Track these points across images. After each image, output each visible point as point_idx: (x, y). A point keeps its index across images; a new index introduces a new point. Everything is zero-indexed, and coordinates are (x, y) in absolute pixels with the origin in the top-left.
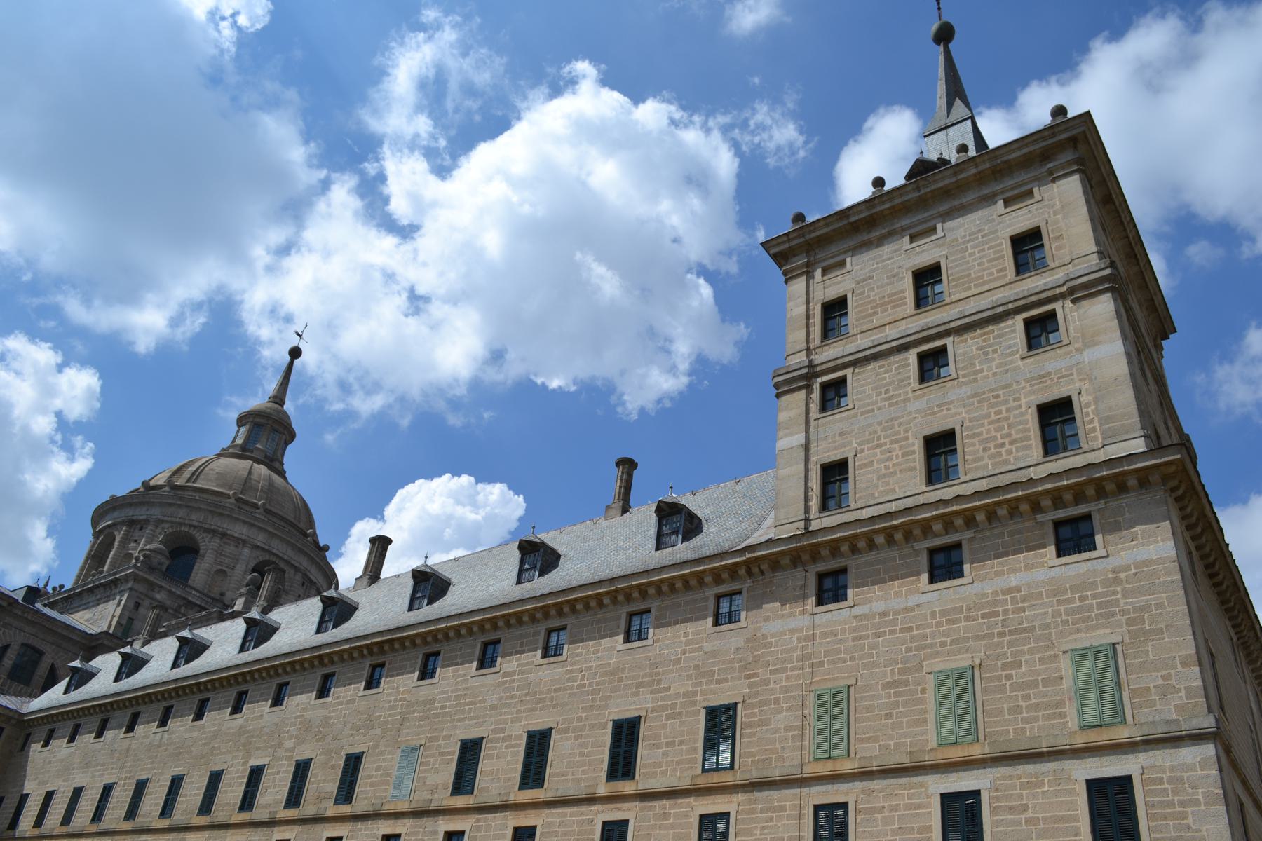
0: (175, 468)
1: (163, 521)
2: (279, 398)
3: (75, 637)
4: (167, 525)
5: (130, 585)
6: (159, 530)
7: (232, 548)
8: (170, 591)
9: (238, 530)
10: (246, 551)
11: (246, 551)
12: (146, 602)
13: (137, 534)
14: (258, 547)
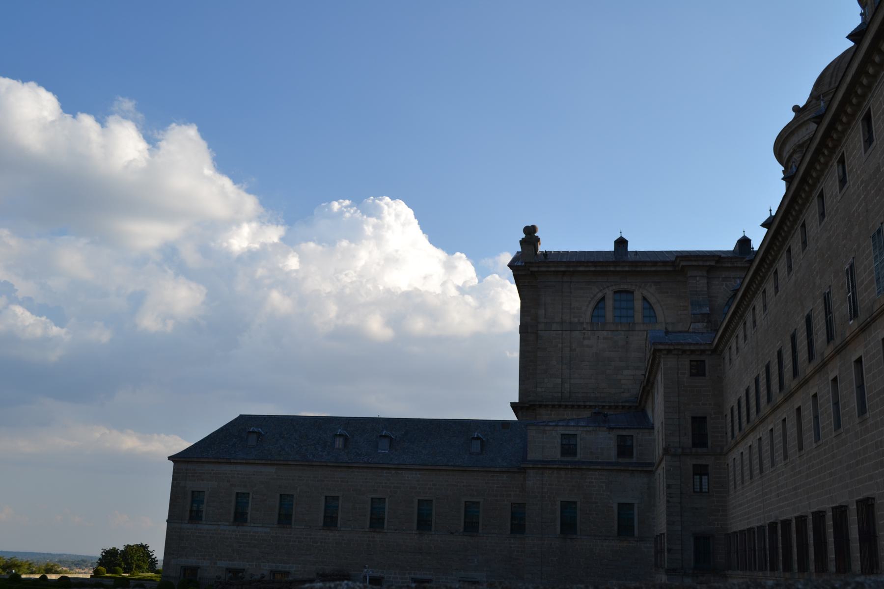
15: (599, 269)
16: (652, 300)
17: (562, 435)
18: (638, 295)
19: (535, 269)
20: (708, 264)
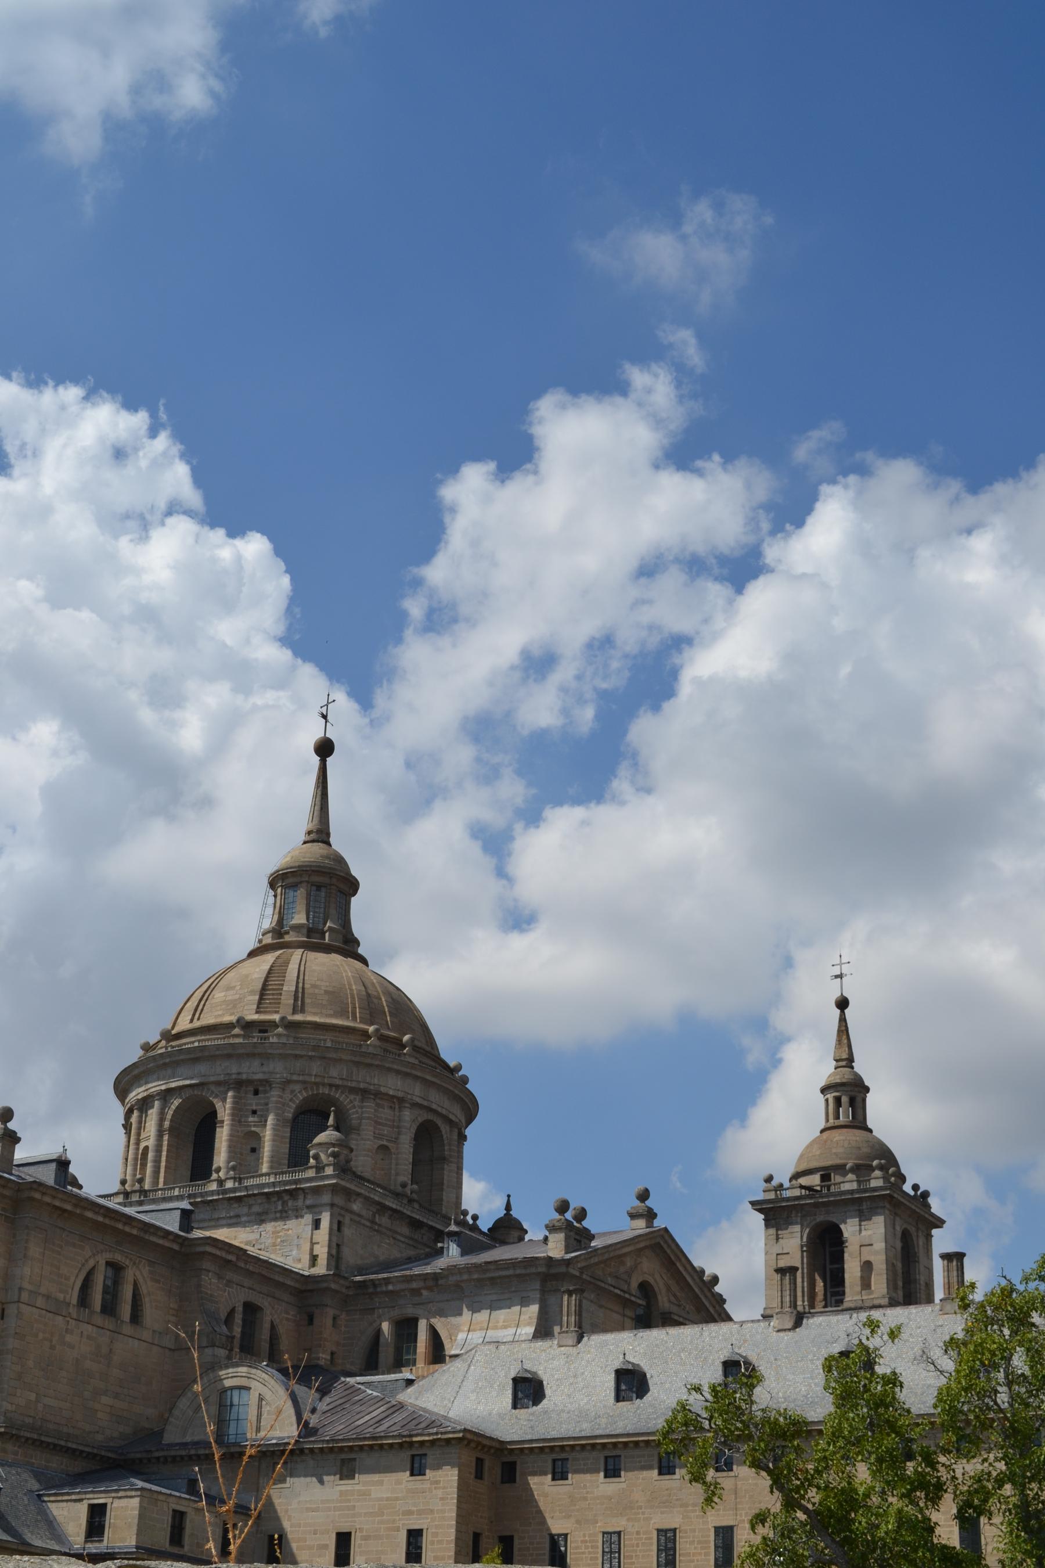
0: (260, 986)
1: (289, 1082)
2: (321, 834)
3: (289, 1282)
4: (297, 1087)
5: (326, 1198)
6: (287, 1096)
7: (387, 1111)
8: (367, 1199)
9: (392, 1085)
10: (407, 1114)
11: (407, 1114)
12: (347, 1221)
13: (253, 1102)
14: (415, 1105)
15: (107, 1221)
16: (143, 1290)
17: (174, 1511)
18: (130, 1275)
19: (37, 1196)
20: (230, 1257)
